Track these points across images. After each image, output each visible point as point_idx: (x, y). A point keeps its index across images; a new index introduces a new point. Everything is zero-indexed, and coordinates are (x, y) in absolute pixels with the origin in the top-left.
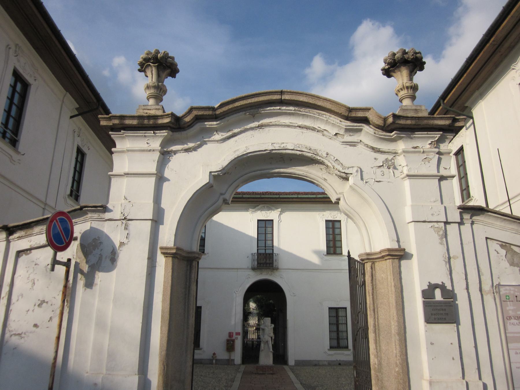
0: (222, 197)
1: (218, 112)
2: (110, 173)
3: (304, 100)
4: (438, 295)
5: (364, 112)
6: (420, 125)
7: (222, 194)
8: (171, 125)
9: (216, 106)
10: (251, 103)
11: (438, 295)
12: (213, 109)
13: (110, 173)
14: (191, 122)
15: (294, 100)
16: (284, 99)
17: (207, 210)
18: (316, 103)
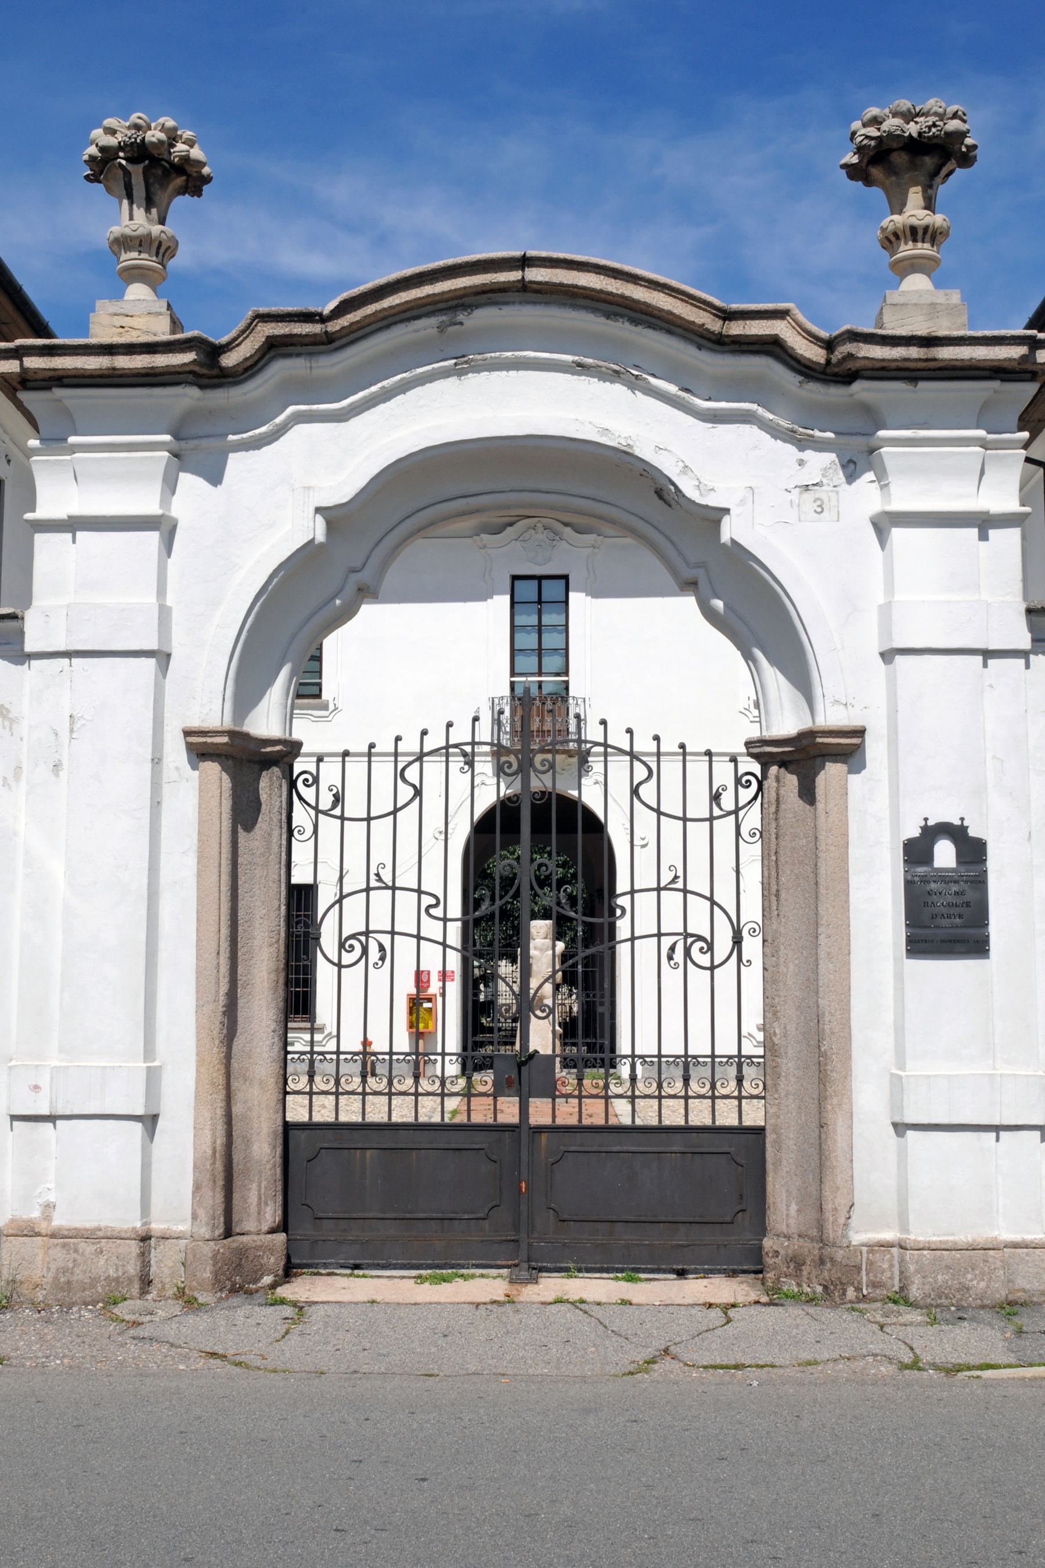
0: (355, 577)
1: (334, 326)
2: (29, 516)
3: (592, 285)
4: (945, 855)
5: (770, 323)
6: (935, 360)
7: (354, 571)
8: (197, 369)
9: (327, 310)
10: (434, 295)
11: (945, 855)
12: (323, 319)
13: (29, 516)
14: (256, 358)
15: (561, 285)
16: (531, 282)
17: (312, 616)
18: (627, 293)
